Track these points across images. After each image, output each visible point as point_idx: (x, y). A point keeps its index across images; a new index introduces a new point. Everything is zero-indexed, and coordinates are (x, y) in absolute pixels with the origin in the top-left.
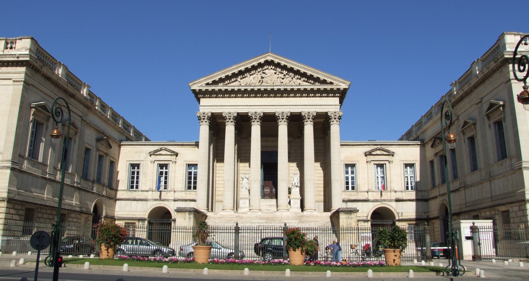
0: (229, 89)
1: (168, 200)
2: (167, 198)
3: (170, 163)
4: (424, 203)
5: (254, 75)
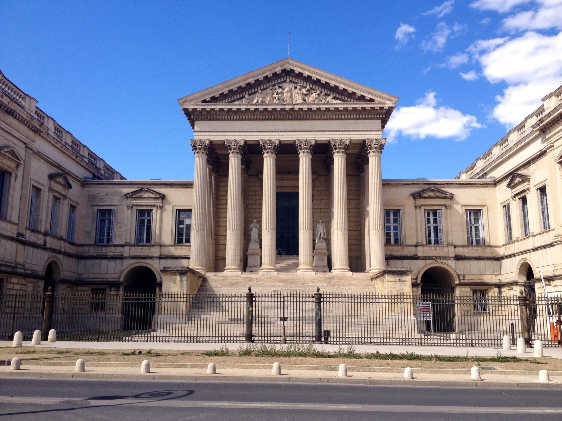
0: (234, 108)
1: (151, 258)
2: (151, 255)
3: (155, 209)
4: (496, 262)
5: (268, 91)
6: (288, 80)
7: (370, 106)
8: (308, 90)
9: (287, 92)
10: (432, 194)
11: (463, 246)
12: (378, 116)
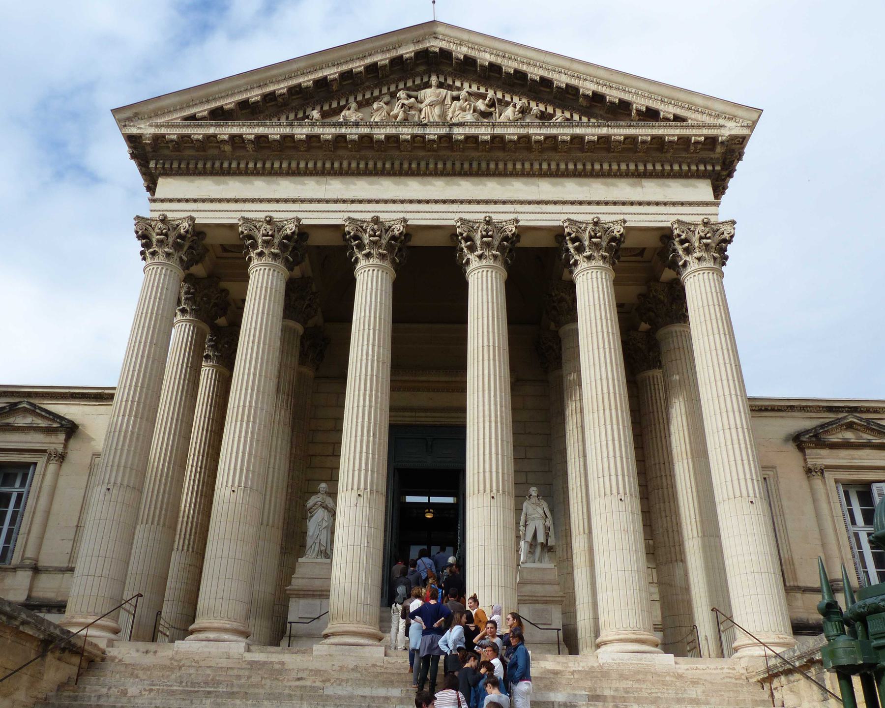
6: (434, 80)
7: (678, 131)
8: (492, 104)
9: (431, 105)
10: (850, 436)
12: (702, 168)
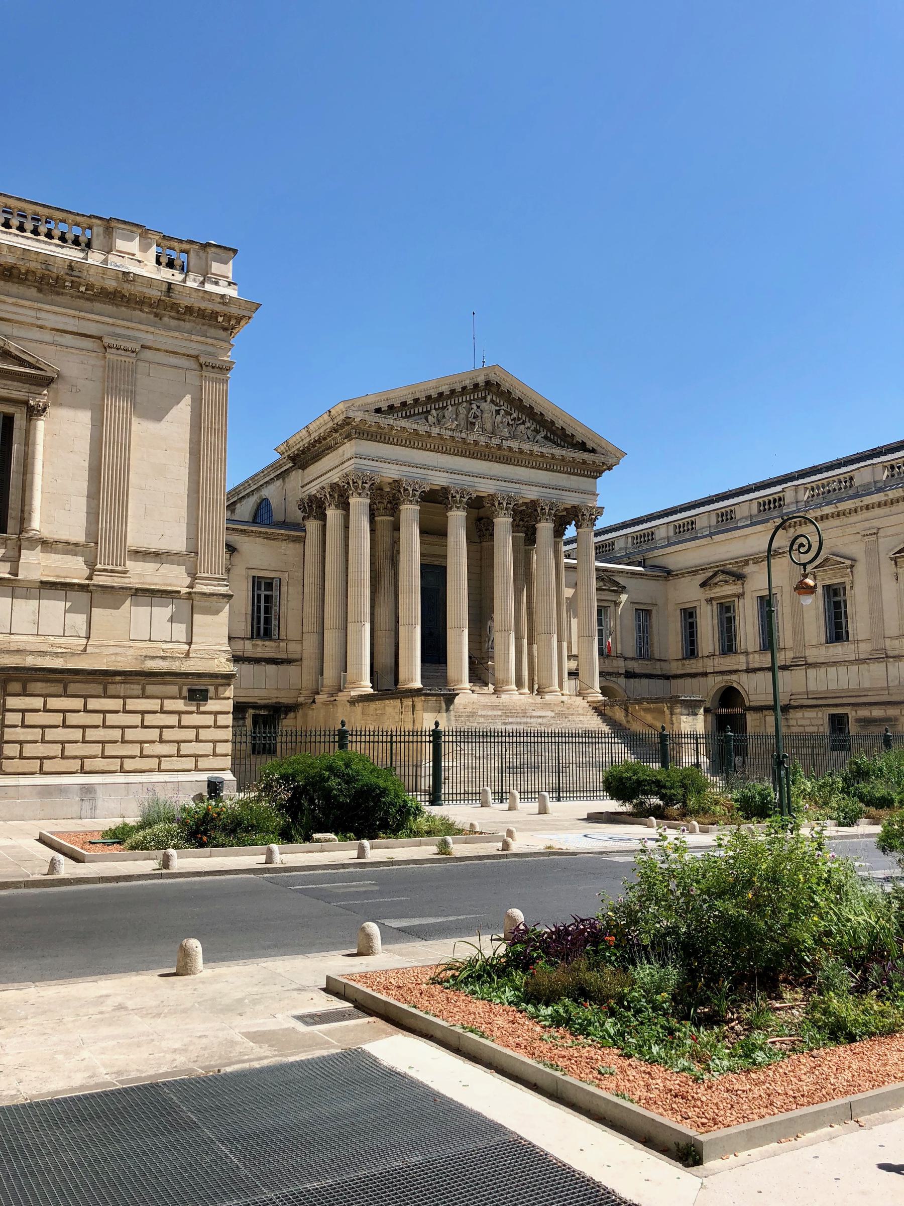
6: (489, 398)
8: (514, 420)
11: (632, 659)
